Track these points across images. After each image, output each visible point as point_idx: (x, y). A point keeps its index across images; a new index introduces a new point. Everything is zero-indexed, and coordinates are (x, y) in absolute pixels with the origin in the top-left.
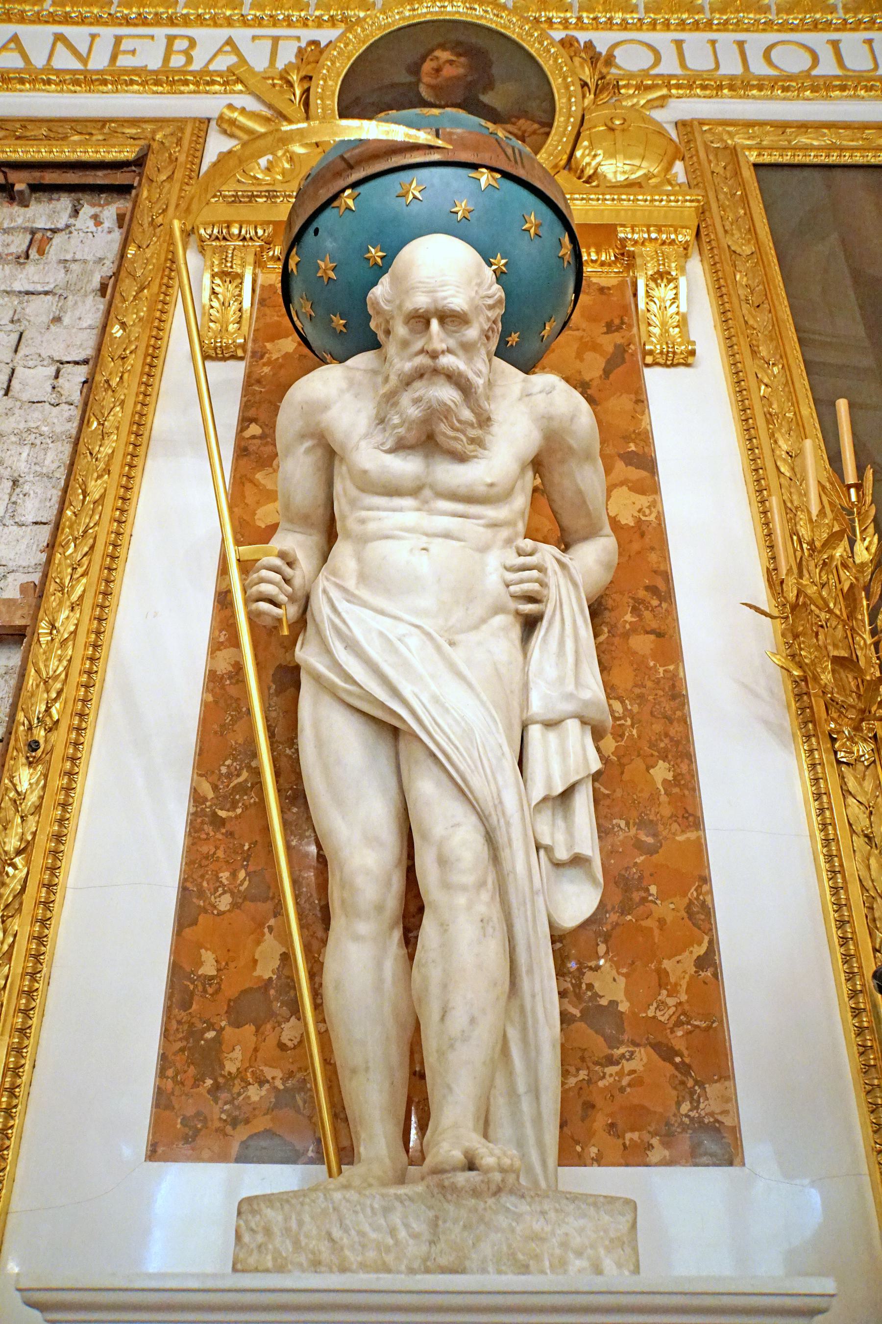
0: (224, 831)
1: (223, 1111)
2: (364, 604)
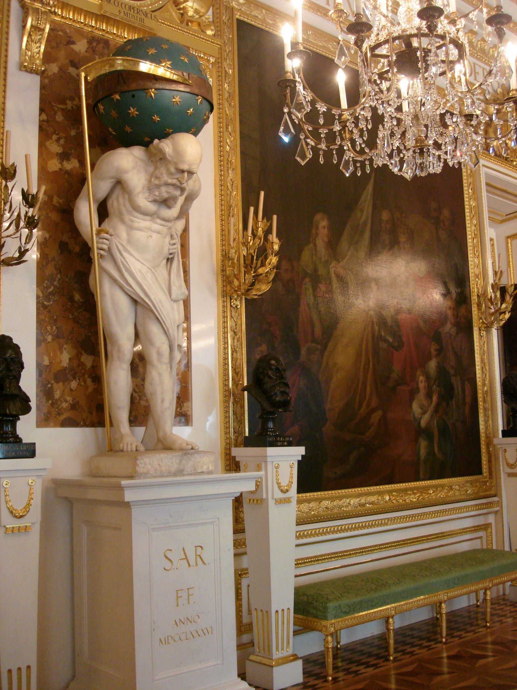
0: (47, 310)
1: (55, 411)
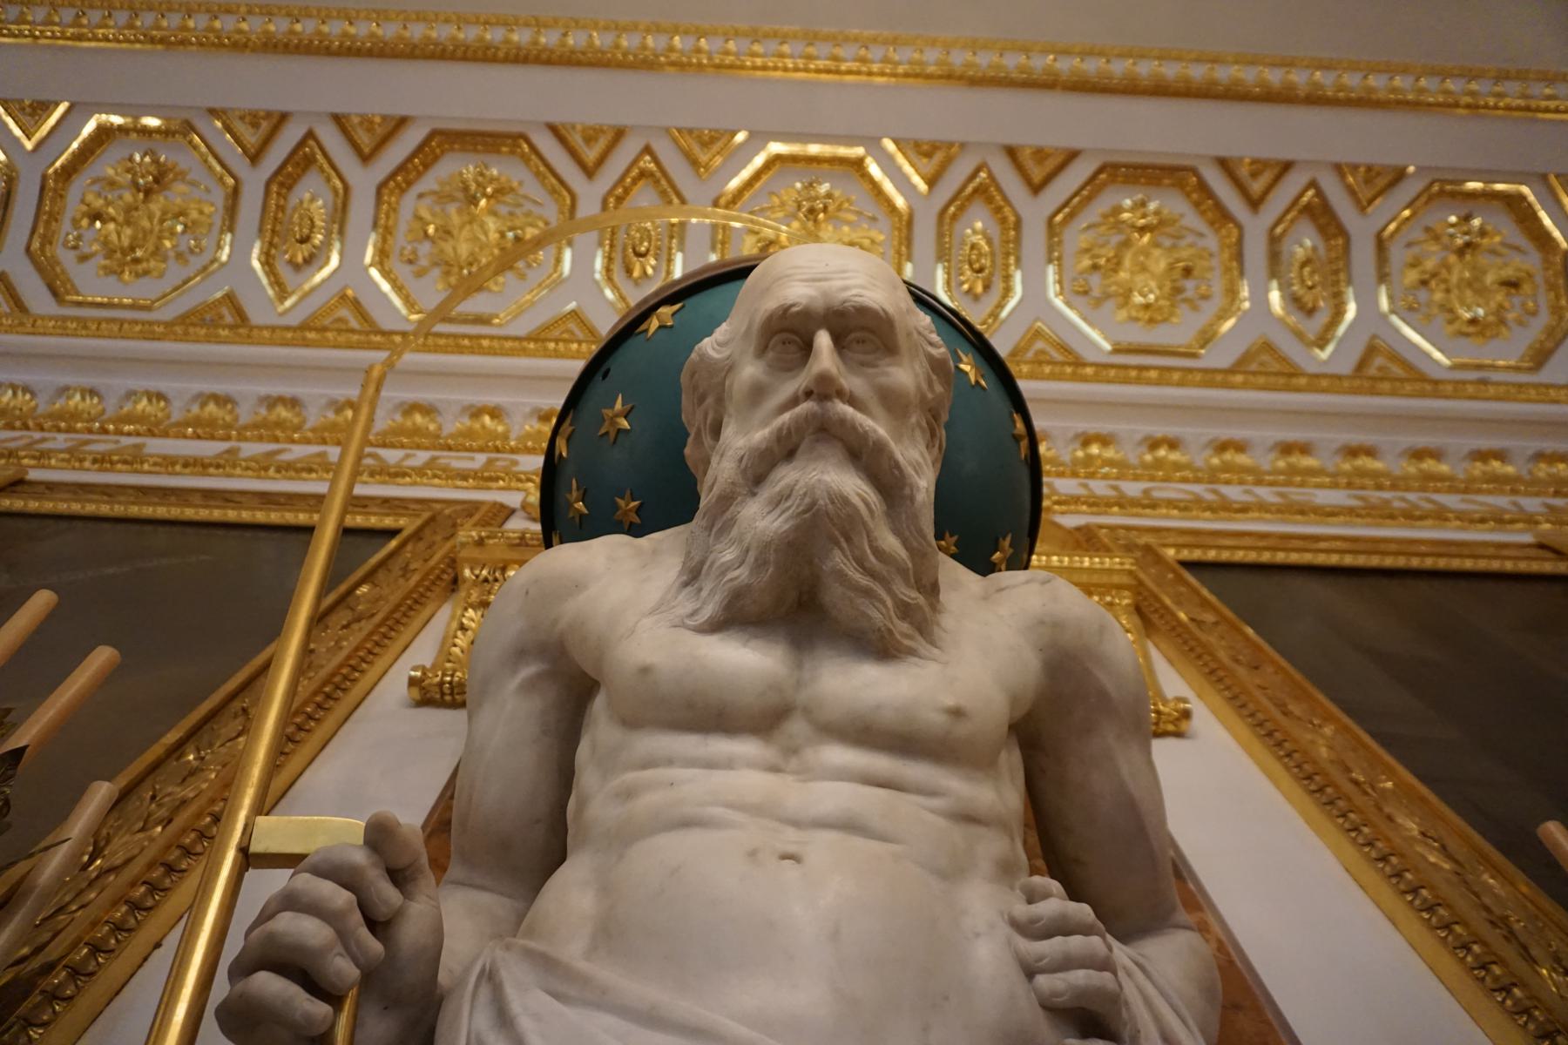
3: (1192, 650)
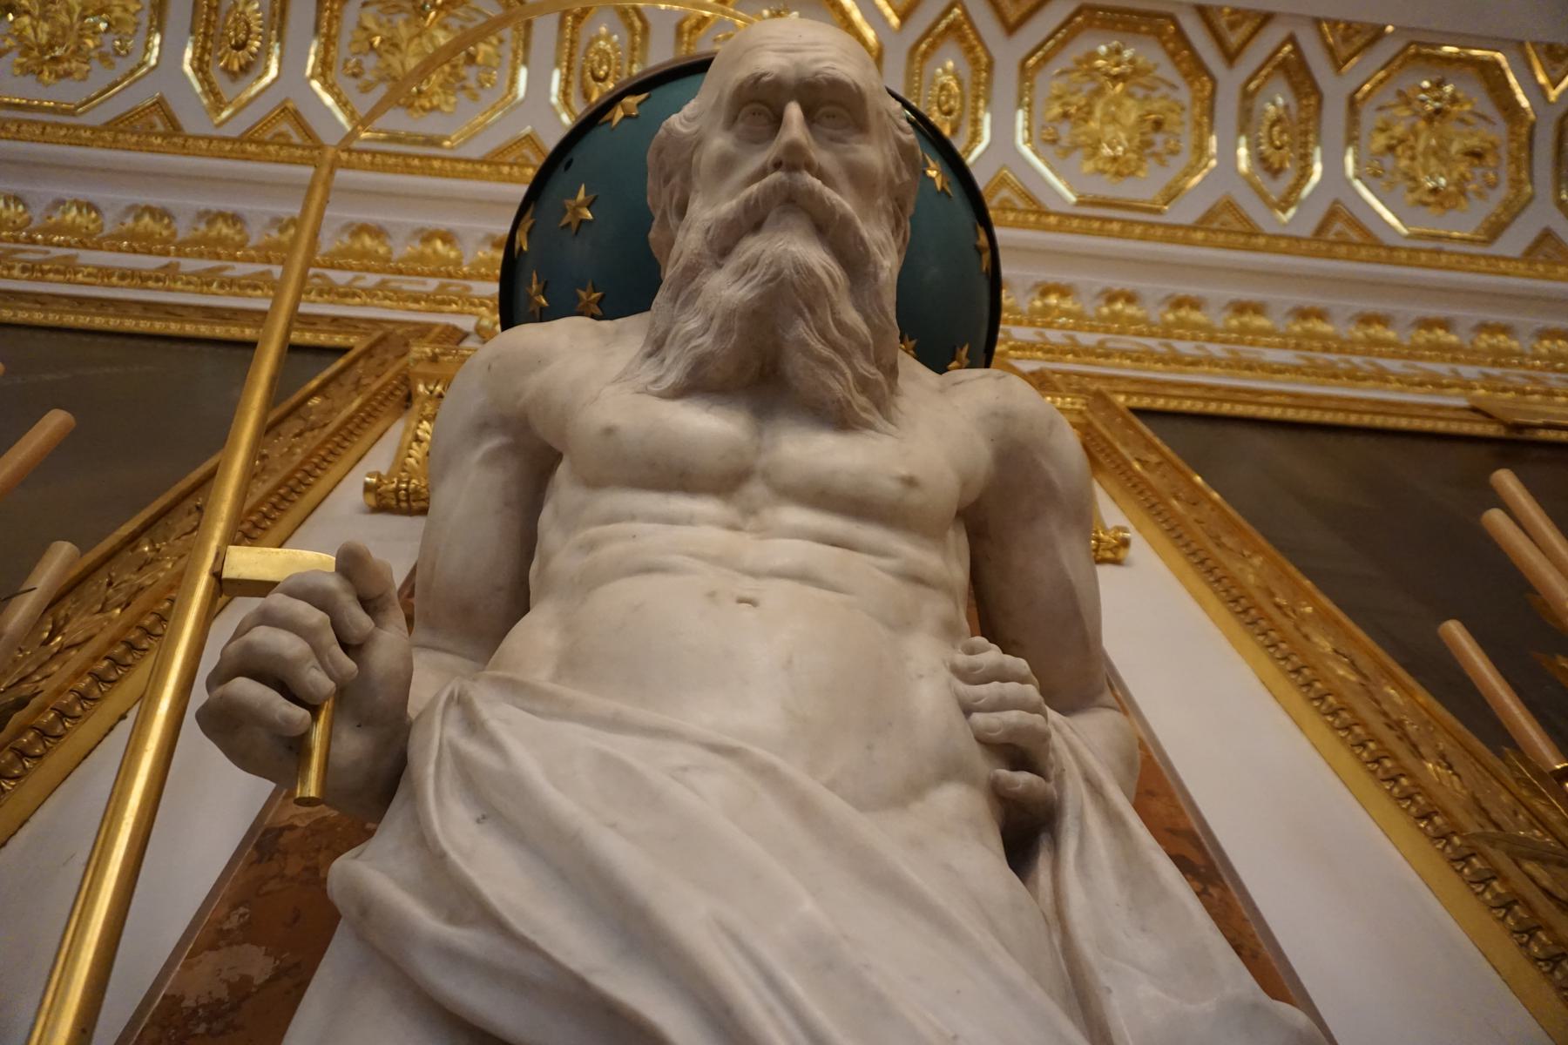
2: (566, 711)
3: (1134, 486)
